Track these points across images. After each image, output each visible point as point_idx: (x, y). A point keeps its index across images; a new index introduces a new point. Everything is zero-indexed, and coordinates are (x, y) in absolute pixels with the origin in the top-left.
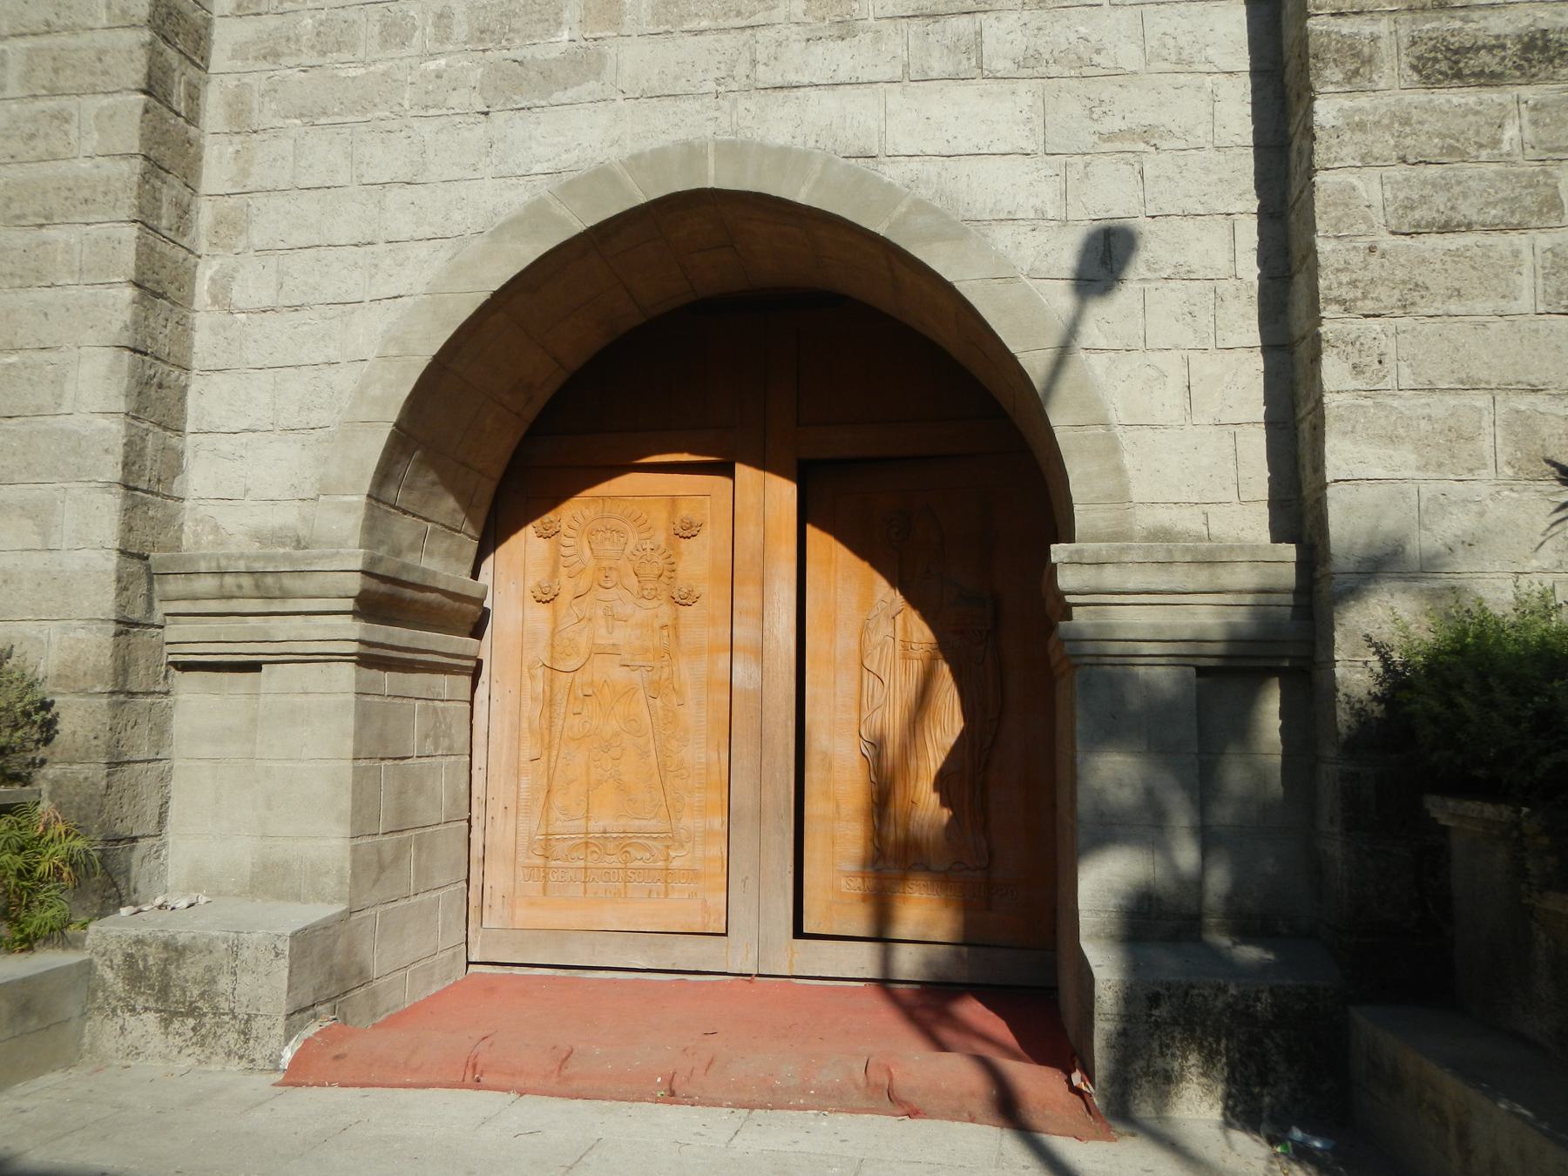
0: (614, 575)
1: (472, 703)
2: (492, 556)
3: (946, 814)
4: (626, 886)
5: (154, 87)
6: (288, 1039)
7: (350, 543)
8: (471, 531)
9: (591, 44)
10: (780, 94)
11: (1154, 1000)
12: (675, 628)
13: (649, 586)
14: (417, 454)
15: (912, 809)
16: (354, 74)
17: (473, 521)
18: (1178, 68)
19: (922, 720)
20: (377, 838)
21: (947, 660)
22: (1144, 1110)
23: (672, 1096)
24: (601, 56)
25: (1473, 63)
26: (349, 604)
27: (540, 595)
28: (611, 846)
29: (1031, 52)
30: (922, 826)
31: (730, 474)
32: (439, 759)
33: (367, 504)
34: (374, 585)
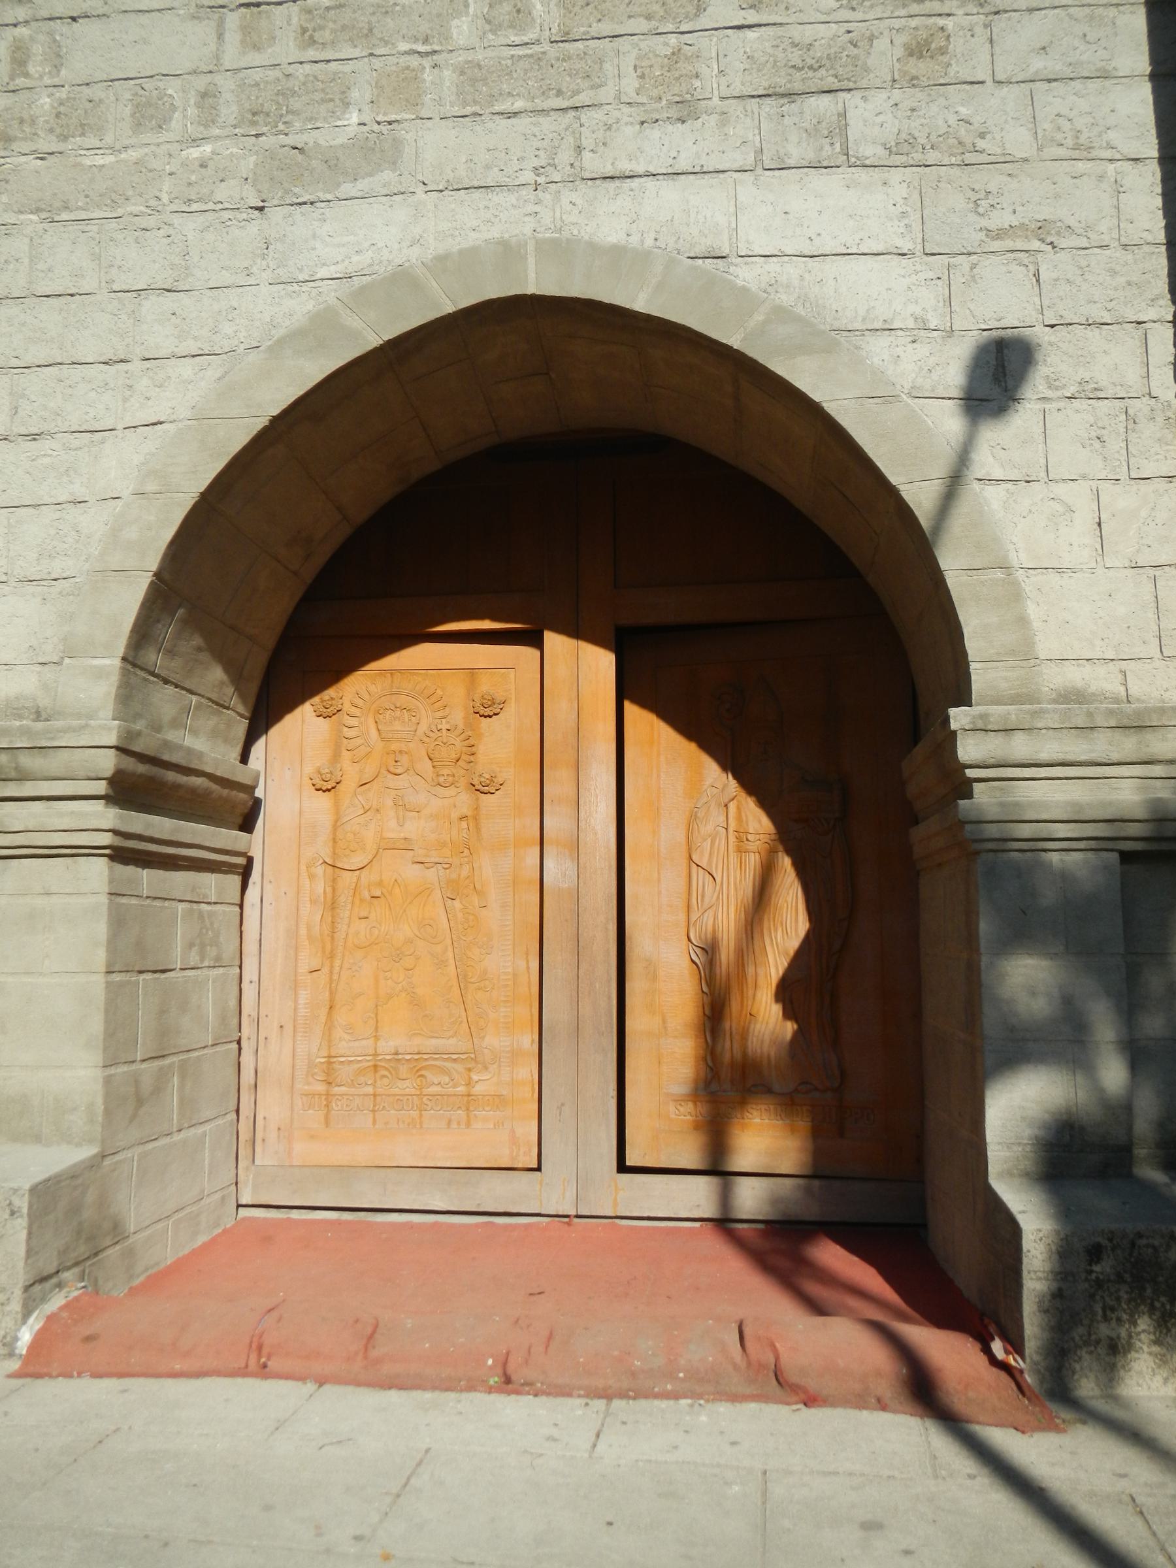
0: (404, 759)
1: (241, 906)
2: (263, 739)
3: (790, 1027)
4: (421, 1116)
6: (26, 1314)
7: (101, 714)
8: (241, 709)
9: (385, 129)
10: (612, 185)
11: (1095, 1253)
12: (476, 818)
13: (446, 771)
14: (181, 612)
15: (750, 1023)
16: (101, 162)
17: (243, 697)
18: (1076, 154)
19: (761, 921)
20: (134, 1067)
21: (788, 852)
22: (1087, 1388)
23: (508, 1383)
24: (397, 144)
26: (101, 788)
27: (320, 784)
28: (403, 1070)
29: (904, 136)
30: (762, 1042)
31: (538, 643)
32: (205, 972)
33: (122, 668)
34: (130, 764)
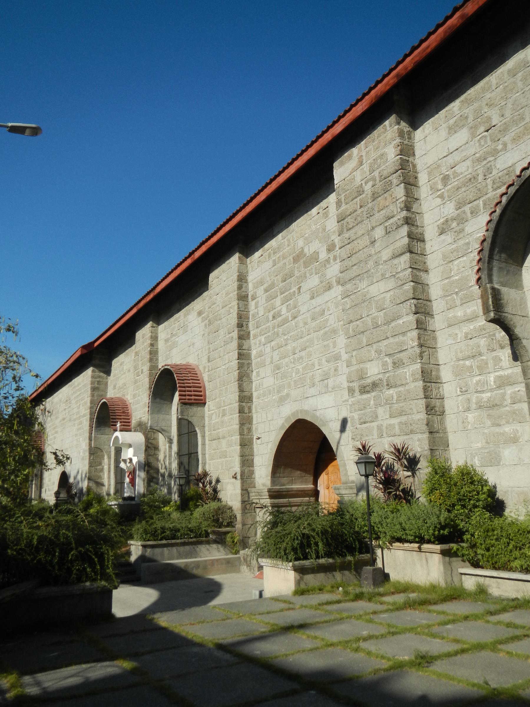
26: (268, 497)
34: (272, 493)
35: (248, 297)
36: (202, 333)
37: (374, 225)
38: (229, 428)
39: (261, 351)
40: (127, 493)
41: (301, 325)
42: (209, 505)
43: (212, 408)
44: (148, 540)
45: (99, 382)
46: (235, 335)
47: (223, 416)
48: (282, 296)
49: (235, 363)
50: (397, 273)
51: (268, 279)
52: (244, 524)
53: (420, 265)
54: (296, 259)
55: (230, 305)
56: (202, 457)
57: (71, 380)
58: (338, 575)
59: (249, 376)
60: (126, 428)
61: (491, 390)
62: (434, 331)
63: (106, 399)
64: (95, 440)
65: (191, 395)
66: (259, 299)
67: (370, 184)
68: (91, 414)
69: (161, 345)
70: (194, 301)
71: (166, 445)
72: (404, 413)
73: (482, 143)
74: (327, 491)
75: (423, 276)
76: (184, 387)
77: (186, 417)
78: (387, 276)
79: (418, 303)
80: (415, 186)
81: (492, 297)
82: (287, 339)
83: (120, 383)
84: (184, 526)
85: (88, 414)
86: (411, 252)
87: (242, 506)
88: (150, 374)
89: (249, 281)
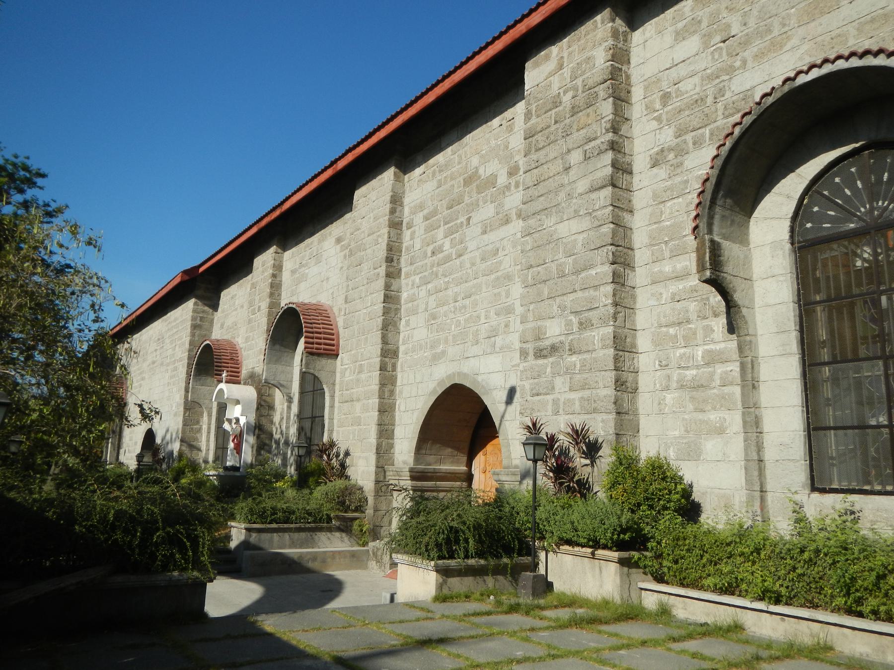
5: (383, 368)
25: (542, 353)
26: (409, 478)
34: (414, 474)
35: (402, 224)
36: (340, 265)
37: (570, 147)
38: (366, 388)
39: (414, 294)
40: (230, 461)
41: (468, 265)
42: (333, 484)
43: (346, 361)
44: (254, 523)
45: (202, 319)
46: (382, 271)
47: (359, 373)
48: (446, 227)
49: (379, 307)
50: (594, 211)
51: (430, 203)
52: (376, 510)
53: (623, 204)
54: (468, 182)
55: (378, 233)
56: (329, 423)
57: (166, 314)
58: (490, 581)
59: (396, 326)
60: (234, 379)
61: (698, 367)
62: (634, 288)
63: (210, 341)
64: (192, 393)
65: (320, 344)
66: (416, 228)
67: (570, 94)
68: (189, 358)
69: (286, 277)
70: (332, 223)
71: (283, 404)
72: (587, 387)
73: (716, 57)
74: (483, 476)
75: (626, 217)
76: (312, 333)
77: (312, 371)
78: (581, 213)
79: (616, 250)
80: (627, 102)
81: (710, 252)
82: (448, 282)
83: (229, 322)
84: (300, 507)
85: (186, 358)
86: (614, 186)
87: (375, 486)
88: (269, 312)
89: (405, 204)
